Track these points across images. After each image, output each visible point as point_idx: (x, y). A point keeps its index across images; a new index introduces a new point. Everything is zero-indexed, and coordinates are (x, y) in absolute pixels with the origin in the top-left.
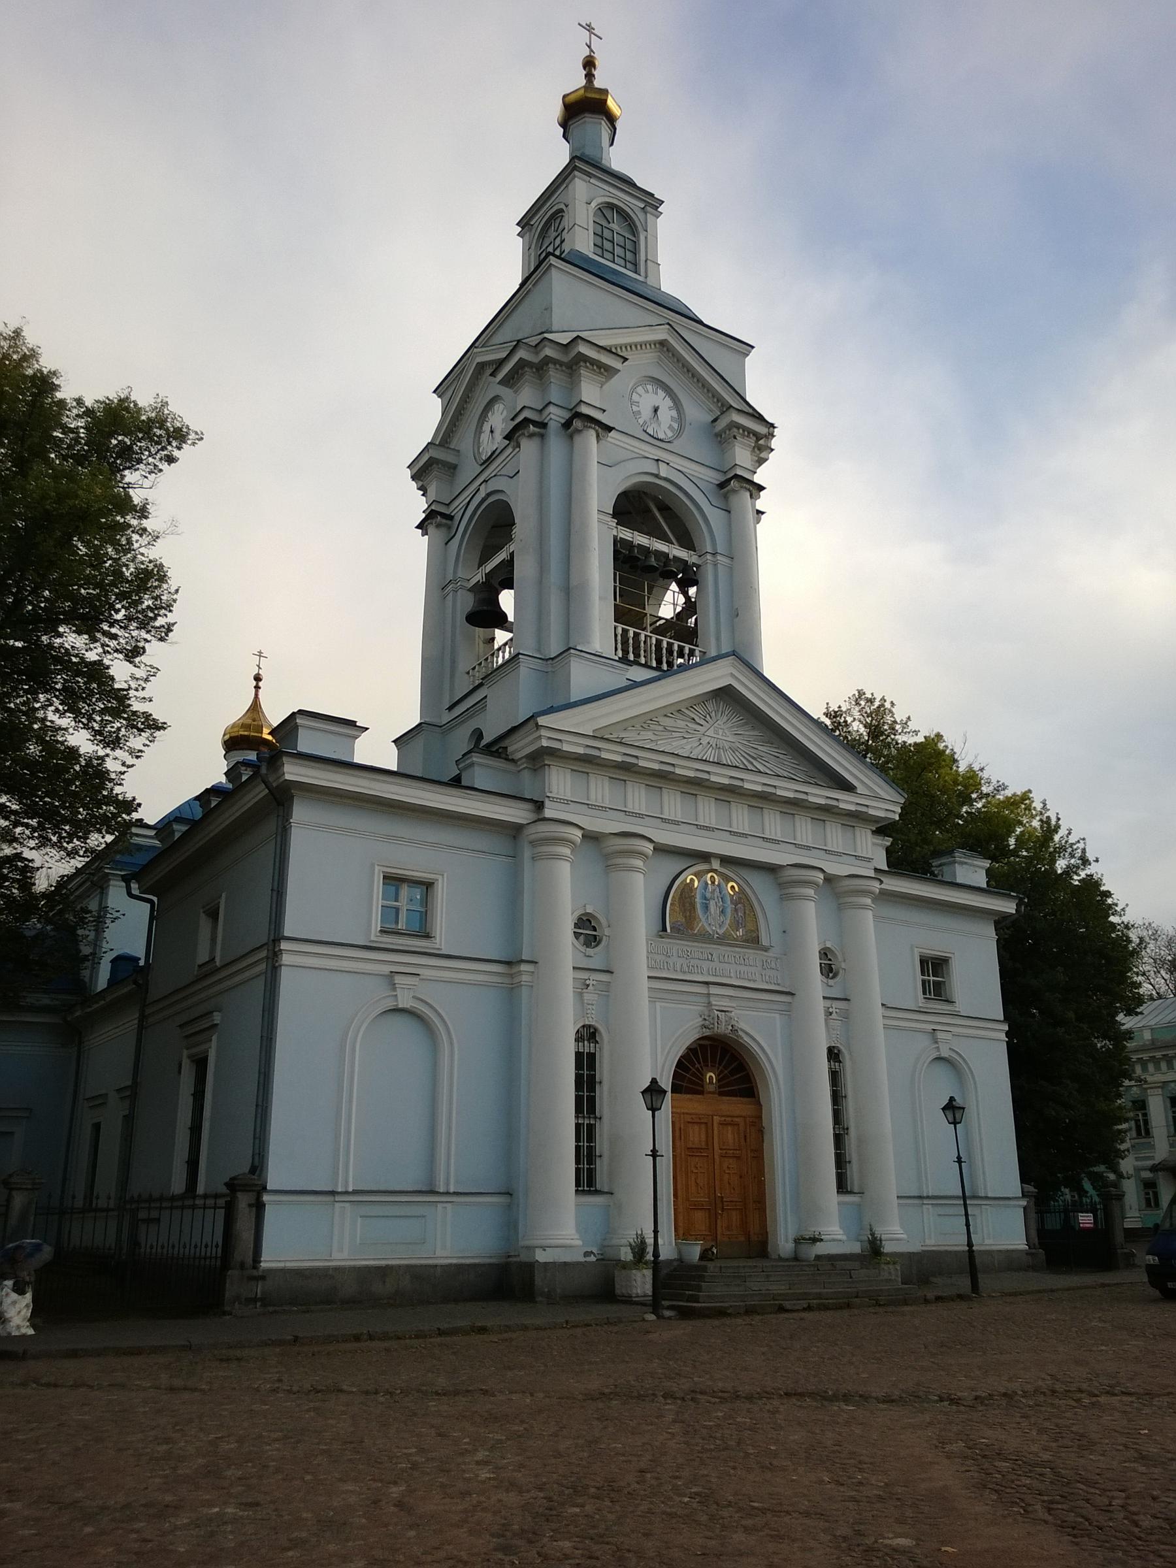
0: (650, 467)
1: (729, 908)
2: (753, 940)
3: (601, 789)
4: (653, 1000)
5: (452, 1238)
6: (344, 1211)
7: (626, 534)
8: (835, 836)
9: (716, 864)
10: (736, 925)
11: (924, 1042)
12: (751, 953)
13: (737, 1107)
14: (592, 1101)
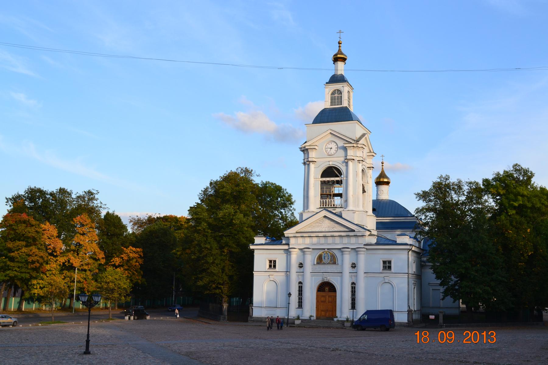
0: (328, 163)
1: (330, 257)
2: (335, 263)
3: (300, 240)
4: (312, 276)
5: (280, 314)
6: (263, 309)
7: (324, 179)
8: (353, 240)
9: (326, 250)
10: (331, 261)
11: (383, 279)
12: (334, 266)
13: (332, 294)
14: (301, 294)
